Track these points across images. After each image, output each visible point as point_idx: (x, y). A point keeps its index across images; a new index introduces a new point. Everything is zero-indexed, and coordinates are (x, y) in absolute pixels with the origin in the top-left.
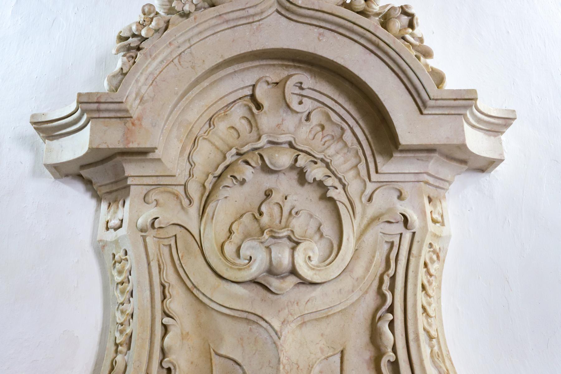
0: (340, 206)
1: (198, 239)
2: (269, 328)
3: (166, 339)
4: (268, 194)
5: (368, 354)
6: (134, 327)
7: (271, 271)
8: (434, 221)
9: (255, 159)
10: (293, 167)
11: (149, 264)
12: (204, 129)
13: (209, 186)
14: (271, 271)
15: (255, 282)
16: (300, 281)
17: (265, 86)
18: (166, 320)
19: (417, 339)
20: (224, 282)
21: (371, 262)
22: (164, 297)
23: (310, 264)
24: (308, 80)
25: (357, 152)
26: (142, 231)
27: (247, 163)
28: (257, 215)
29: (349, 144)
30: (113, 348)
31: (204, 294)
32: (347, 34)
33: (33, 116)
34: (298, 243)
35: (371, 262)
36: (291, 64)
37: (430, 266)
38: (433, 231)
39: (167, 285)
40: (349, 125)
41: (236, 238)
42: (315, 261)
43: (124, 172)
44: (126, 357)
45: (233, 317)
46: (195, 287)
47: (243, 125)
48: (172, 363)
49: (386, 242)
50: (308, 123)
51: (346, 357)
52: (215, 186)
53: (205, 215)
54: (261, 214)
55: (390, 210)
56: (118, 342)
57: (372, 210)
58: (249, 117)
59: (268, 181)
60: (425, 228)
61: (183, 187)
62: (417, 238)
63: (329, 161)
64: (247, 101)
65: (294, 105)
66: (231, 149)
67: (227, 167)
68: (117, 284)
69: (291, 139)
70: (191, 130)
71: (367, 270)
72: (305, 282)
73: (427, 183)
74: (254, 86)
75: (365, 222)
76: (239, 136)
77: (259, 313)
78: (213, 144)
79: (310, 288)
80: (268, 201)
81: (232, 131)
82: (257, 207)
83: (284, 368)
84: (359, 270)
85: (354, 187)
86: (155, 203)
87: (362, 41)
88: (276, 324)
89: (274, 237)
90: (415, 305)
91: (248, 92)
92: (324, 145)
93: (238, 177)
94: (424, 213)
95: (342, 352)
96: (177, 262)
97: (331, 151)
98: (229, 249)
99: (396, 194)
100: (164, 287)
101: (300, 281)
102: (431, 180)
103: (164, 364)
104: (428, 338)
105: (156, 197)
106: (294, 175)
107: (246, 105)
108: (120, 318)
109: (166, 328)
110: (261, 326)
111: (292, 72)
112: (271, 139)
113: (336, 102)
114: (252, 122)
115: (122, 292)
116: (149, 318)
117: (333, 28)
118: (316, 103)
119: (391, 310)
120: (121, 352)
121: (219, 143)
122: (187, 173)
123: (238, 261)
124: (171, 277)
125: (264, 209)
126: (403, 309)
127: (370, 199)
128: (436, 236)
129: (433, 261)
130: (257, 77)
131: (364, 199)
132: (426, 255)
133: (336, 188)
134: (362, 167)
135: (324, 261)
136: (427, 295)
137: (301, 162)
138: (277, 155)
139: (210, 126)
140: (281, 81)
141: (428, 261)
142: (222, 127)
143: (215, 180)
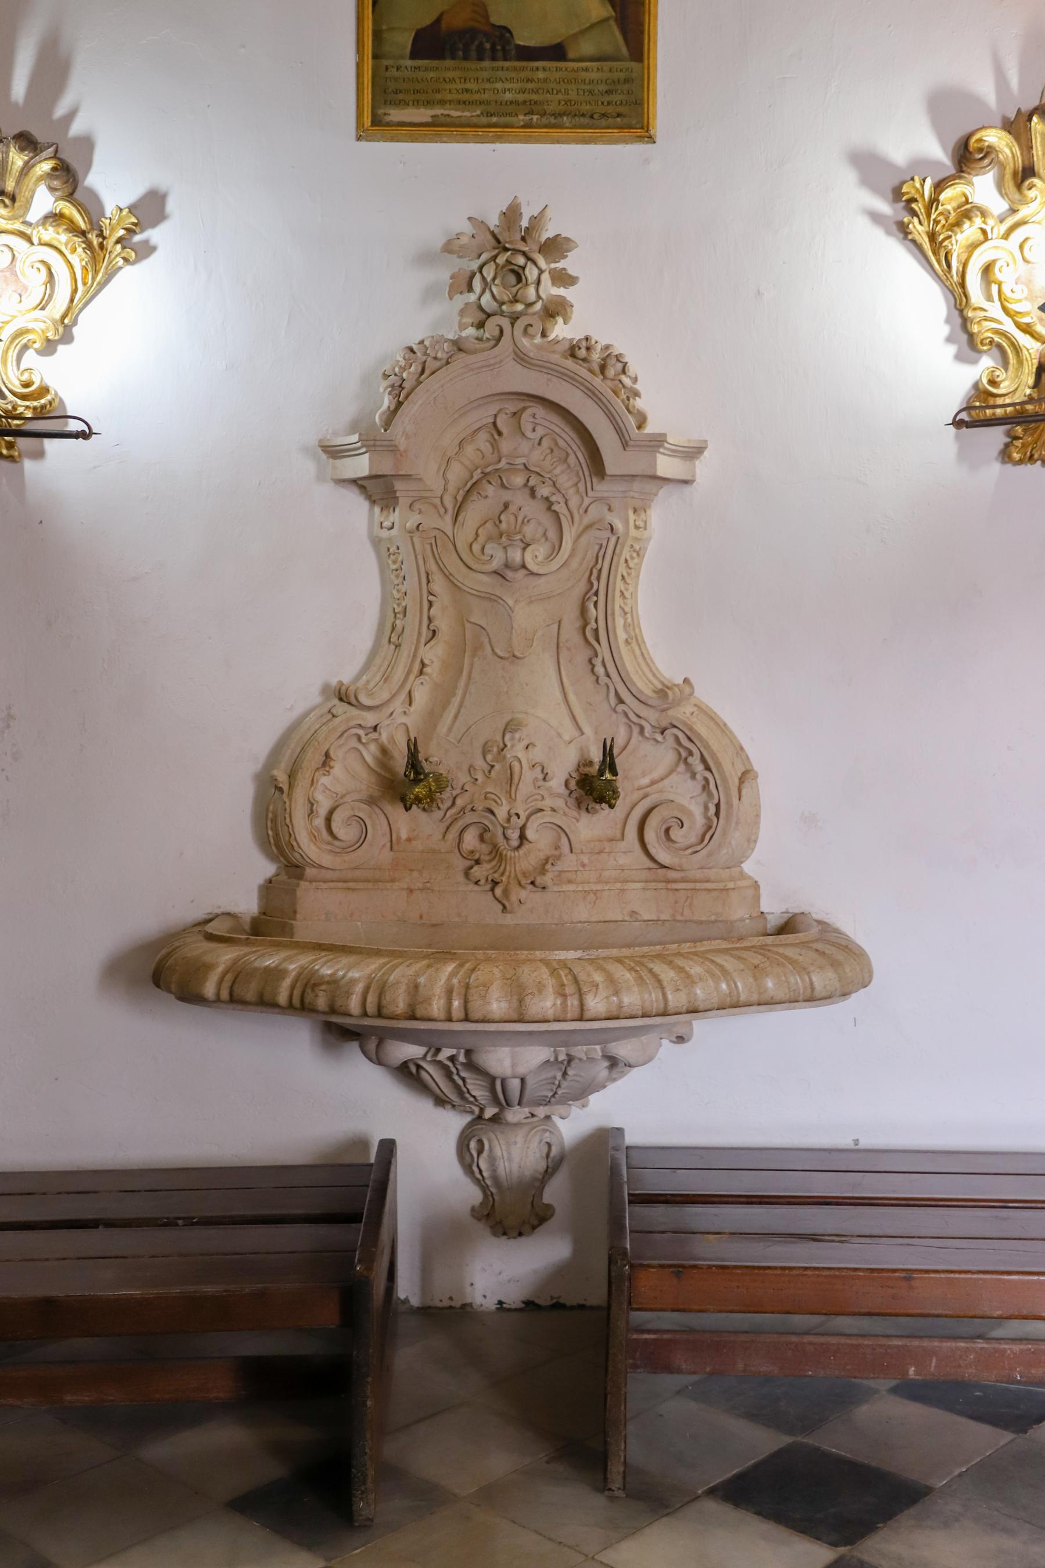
0: (562, 517)
1: (452, 539)
2: (505, 605)
3: (432, 610)
4: (506, 506)
5: (578, 624)
6: (407, 602)
7: (507, 566)
8: (637, 527)
9: (495, 480)
10: (526, 485)
11: (416, 557)
12: (455, 451)
13: (460, 498)
14: (507, 566)
15: (495, 572)
16: (529, 573)
17: (504, 416)
18: (431, 598)
19: (613, 614)
20: (471, 571)
21: (584, 559)
22: (429, 582)
23: (537, 561)
24: (540, 411)
25: (578, 473)
26: (410, 532)
27: (490, 483)
28: (497, 522)
29: (572, 466)
30: (393, 615)
31: (457, 580)
32: (570, 380)
33: (320, 441)
34: (529, 545)
35: (584, 559)
36: (526, 398)
37: (630, 562)
38: (634, 535)
39: (430, 572)
40: (573, 450)
41: (481, 539)
42: (540, 558)
43: (393, 487)
44: (403, 622)
45: (479, 596)
46: (451, 574)
47: (486, 448)
48: (436, 627)
49: (597, 544)
50: (539, 447)
51: (562, 625)
52: (465, 498)
53: (458, 523)
54: (500, 522)
55: (600, 520)
56: (396, 611)
57: (586, 521)
58: (492, 441)
59: (506, 496)
60: (627, 533)
61: (439, 499)
62: (620, 541)
63: (555, 480)
64: (491, 426)
65: (529, 434)
66: (476, 469)
67: (475, 483)
68: (393, 570)
69: (525, 461)
70: (444, 453)
71: (581, 564)
72: (532, 574)
73: (633, 497)
74: (496, 416)
75: (581, 528)
76: (483, 457)
77: (498, 595)
78: (462, 463)
79: (536, 578)
80: (506, 512)
81: (478, 452)
82: (498, 515)
83: (516, 631)
84: (574, 564)
85: (574, 502)
86: (418, 511)
87: (581, 388)
88: (511, 602)
89: (510, 540)
90: (614, 590)
91: (492, 420)
92: (552, 465)
93: (483, 494)
94: (626, 522)
95: (560, 622)
96: (437, 556)
97: (557, 471)
98: (476, 547)
99: (606, 509)
100: (428, 574)
101: (529, 573)
102: (636, 495)
103: (430, 627)
104: (623, 614)
105: (420, 507)
106: (527, 491)
107: (489, 432)
108: (397, 595)
109: (431, 604)
110: (500, 604)
111: (528, 404)
112: (509, 461)
113: (563, 430)
114: (494, 444)
115: (397, 576)
116: (419, 596)
117: (559, 375)
118: (547, 430)
119: (596, 594)
120: (399, 618)
121: (467, 463)
122: (442, 487)
123: (482, 557)
124: (433, 567)
125: (503, 517)
126: (605, 592)
127: (586, 511)
128: (637, 539)
129: (632, 558)
130: (498, 408)
131: (582, 511)
132: (626, 553)
133: (559, 503)
134: (581, 486)
135: (548, 558)
136: (626, 583)
137: (531, 483)
138: (513, 477)
139: (460, 449)
140: (518, 411)
141: (628, 558)
142: (469, 449)
143: (464, 493)
